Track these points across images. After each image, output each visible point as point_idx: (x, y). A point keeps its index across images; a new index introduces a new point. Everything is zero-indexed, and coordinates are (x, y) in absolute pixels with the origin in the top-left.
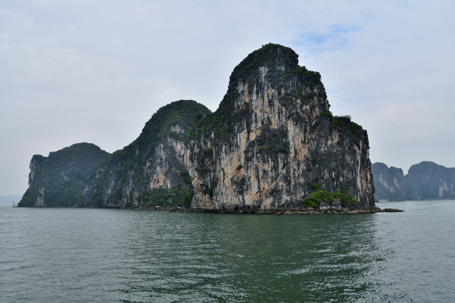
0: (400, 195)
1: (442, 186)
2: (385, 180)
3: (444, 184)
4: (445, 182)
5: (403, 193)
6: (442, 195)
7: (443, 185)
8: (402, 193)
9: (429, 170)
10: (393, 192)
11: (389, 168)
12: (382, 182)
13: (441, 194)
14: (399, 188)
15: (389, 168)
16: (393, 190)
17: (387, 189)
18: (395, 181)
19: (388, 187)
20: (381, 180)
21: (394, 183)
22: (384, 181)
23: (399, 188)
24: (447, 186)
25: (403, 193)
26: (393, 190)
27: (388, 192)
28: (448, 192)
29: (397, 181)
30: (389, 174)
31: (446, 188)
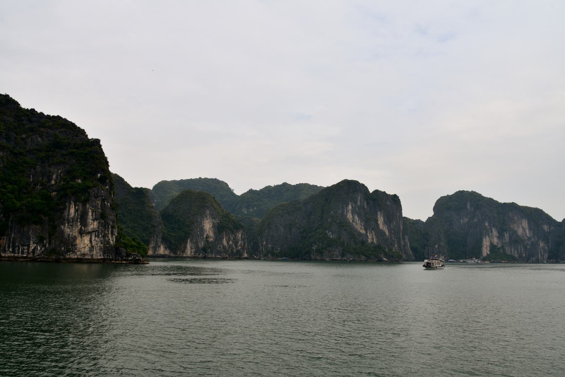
0: (387, 250)
1: (489, 236)
2: (358, 216)
3: (492, 232)
4: (494, 230)
5: (396, 246)
6: (487, 254)
7: (490, 234)
8: (394, 246)
9: (468, 207)
10: (372, 243)
11: (371, 192)
12: (351, 221)
13: (486, 251)
14: (387, 233)
15: (371, 192)
16: (373, 239)
17: (360, 234)
18: (381, 220)
19: (363, 231)
20: (350, 216)
21: (378, 225)
22: (356, 217)
23: (387, 233)
24: (498, 237)
25: (396, 246)
26: (373, 239)
27: (363, 243)
28: (499, 249)
29: (384, 220)
30: (368, 204)
31: (495, 241)
